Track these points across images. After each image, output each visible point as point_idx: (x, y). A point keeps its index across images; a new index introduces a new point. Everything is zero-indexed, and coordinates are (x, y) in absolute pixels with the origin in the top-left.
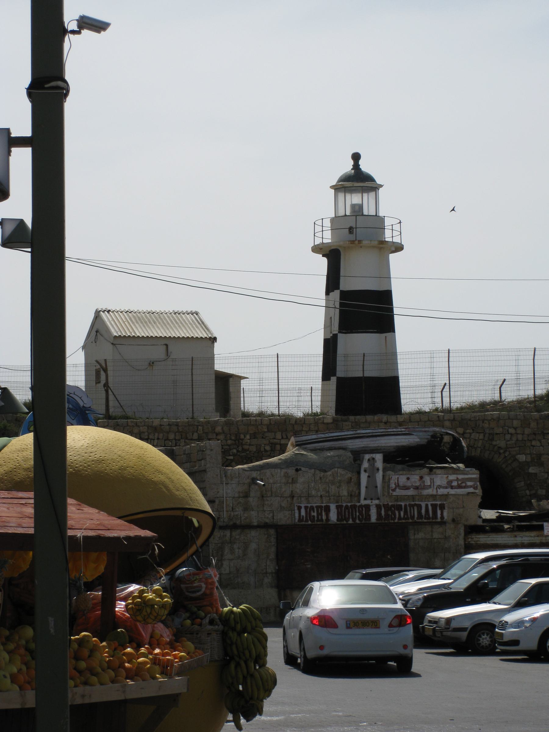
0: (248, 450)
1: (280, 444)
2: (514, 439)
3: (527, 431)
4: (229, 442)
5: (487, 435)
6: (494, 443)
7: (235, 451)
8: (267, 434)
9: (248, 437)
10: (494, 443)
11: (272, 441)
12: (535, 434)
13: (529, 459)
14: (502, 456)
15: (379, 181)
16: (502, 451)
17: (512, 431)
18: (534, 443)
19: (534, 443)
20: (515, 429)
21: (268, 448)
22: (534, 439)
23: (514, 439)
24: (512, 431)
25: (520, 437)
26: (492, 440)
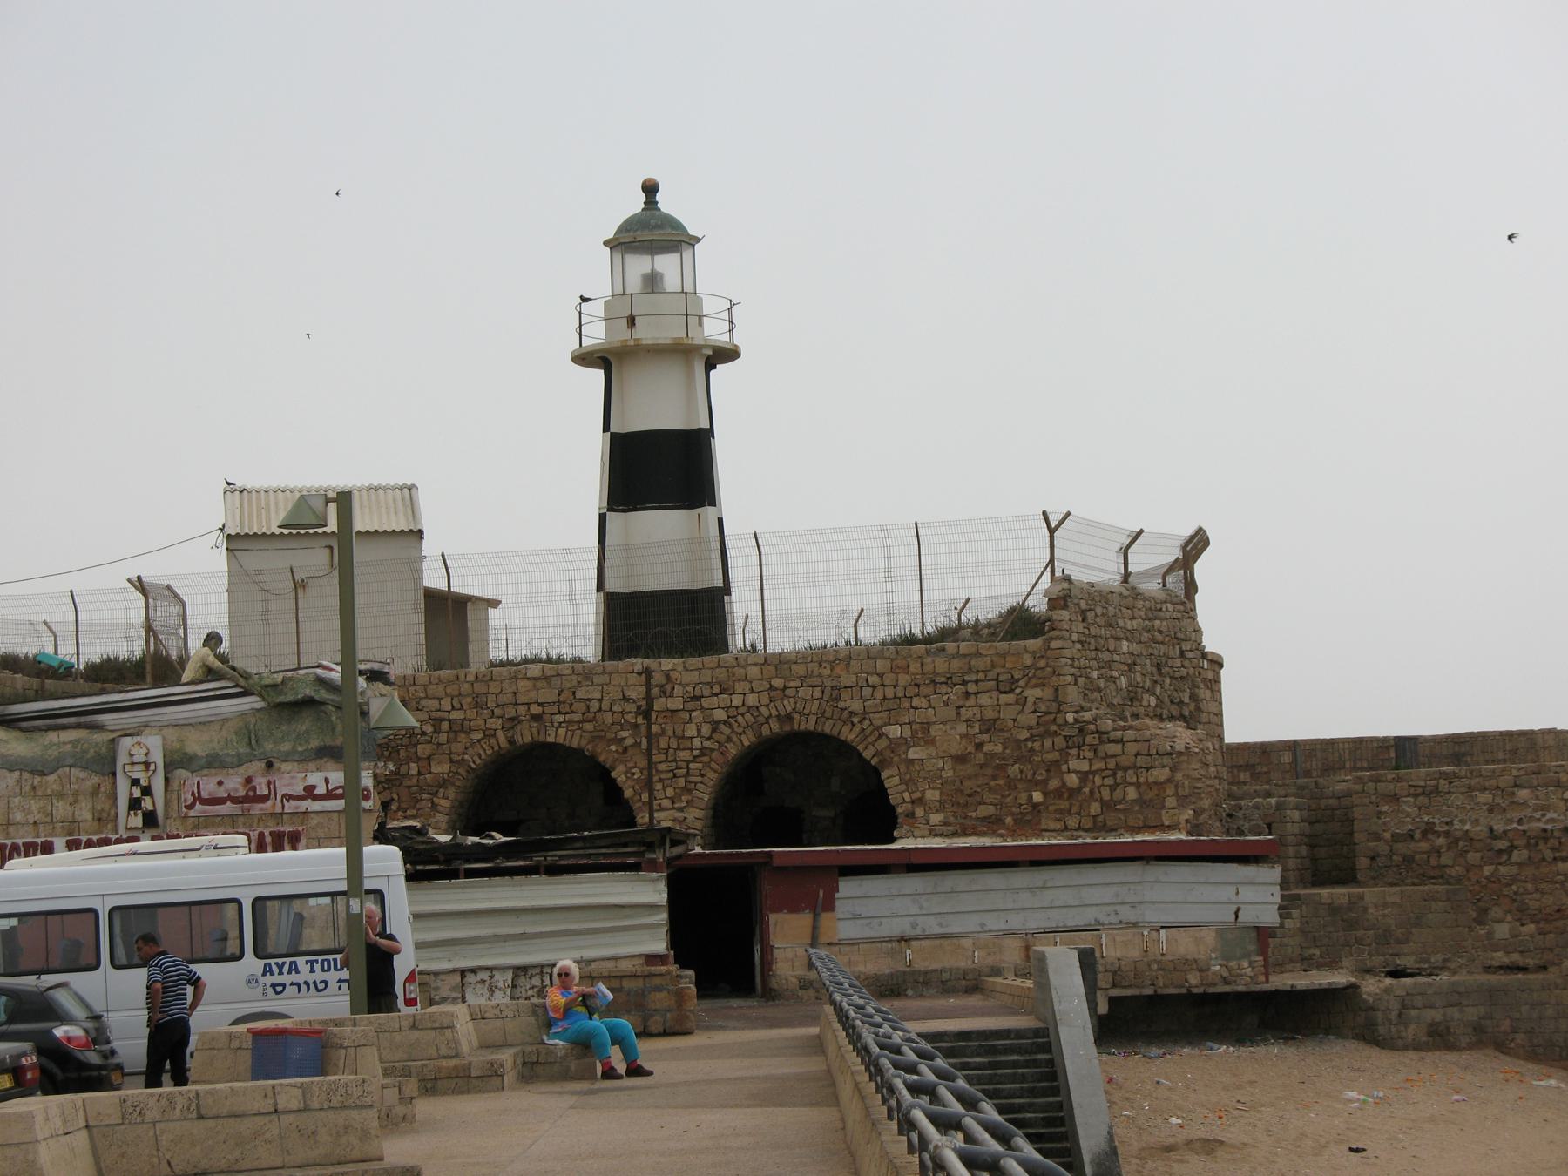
2: (879, 694)
3: (904, 679)
5: (828, 690)
6: (841, 705)
8: (424, 702)
11: (434, 715)
12: (917, 685)
13: (907, 733)
14: (857, 729)
15: (692, 231)
16: (855, 720)
17: (873, 680)
18: (916, 702)
19: (916, 702)
20: (881, 676)
21: (428, 728)
22: (917, 695)
23: (879, 694)
25: (890, 692)
26: (838, 699)
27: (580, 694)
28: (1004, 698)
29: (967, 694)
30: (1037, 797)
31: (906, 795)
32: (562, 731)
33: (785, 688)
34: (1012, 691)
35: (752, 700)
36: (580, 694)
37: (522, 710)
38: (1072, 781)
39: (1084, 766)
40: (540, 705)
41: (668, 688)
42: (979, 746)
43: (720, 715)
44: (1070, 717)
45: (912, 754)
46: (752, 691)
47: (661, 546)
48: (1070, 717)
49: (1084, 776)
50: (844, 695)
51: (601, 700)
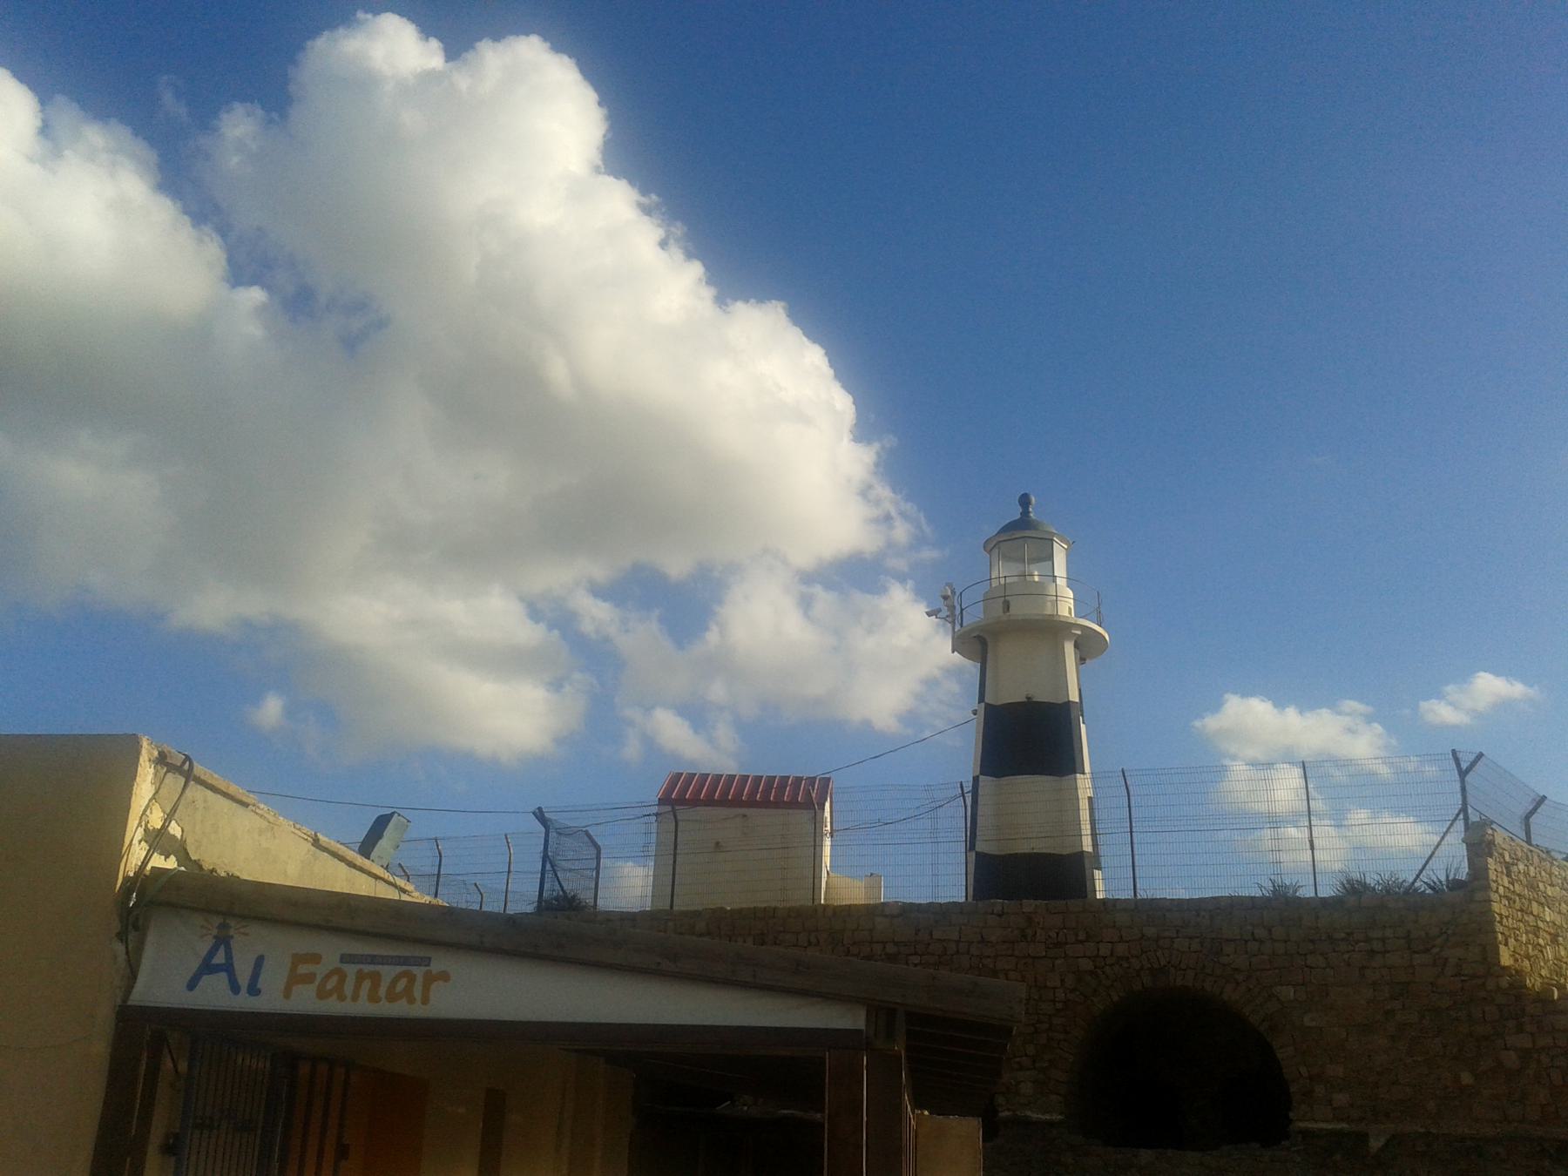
12: (1312, 941)
16: (1240, 978)
27: (937, 935)
31: (1303, 1070)
34: (1427, 951)
35: (1121, 949)
41: (1030, 932)
43: (1086, 965)
45: (1307, 1021)
46: (1121, 940)
47: (1026, 814)
51: (958, 942)
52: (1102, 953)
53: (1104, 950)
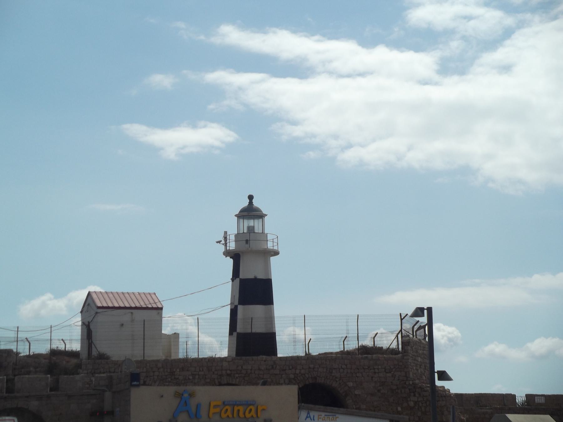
0: (177, 379)
1: (199, 375)
4: (166, 374)
6: (333, 374)
7: (170, 379)
9: (178, 370)
10: (333, 374)
12: (358, 369)
16: (337, 380)
17: (344, 366)
18: (358, 375)
21: (191, 377)
24: (344, 366)
28: (388, 375)
29: (375, 373)
30: (399, 409)
32: (238, 380)
33: (314, 368)
34: (390, 372)
35: (303, 371)
36: (244, 367)
37: (224, 372)
38: (412, 404)
39: (415, 399)
40: (231, 371)
41: (275, 366)
42: (379, 391)
43: (292, 376)
44: (411, 382)
46: (303, 369)
48: (411, 382)
49: (416, 403)
50: (334, 371)
51: (251, 370)
52: (297, 372)
53: (298, 372)
